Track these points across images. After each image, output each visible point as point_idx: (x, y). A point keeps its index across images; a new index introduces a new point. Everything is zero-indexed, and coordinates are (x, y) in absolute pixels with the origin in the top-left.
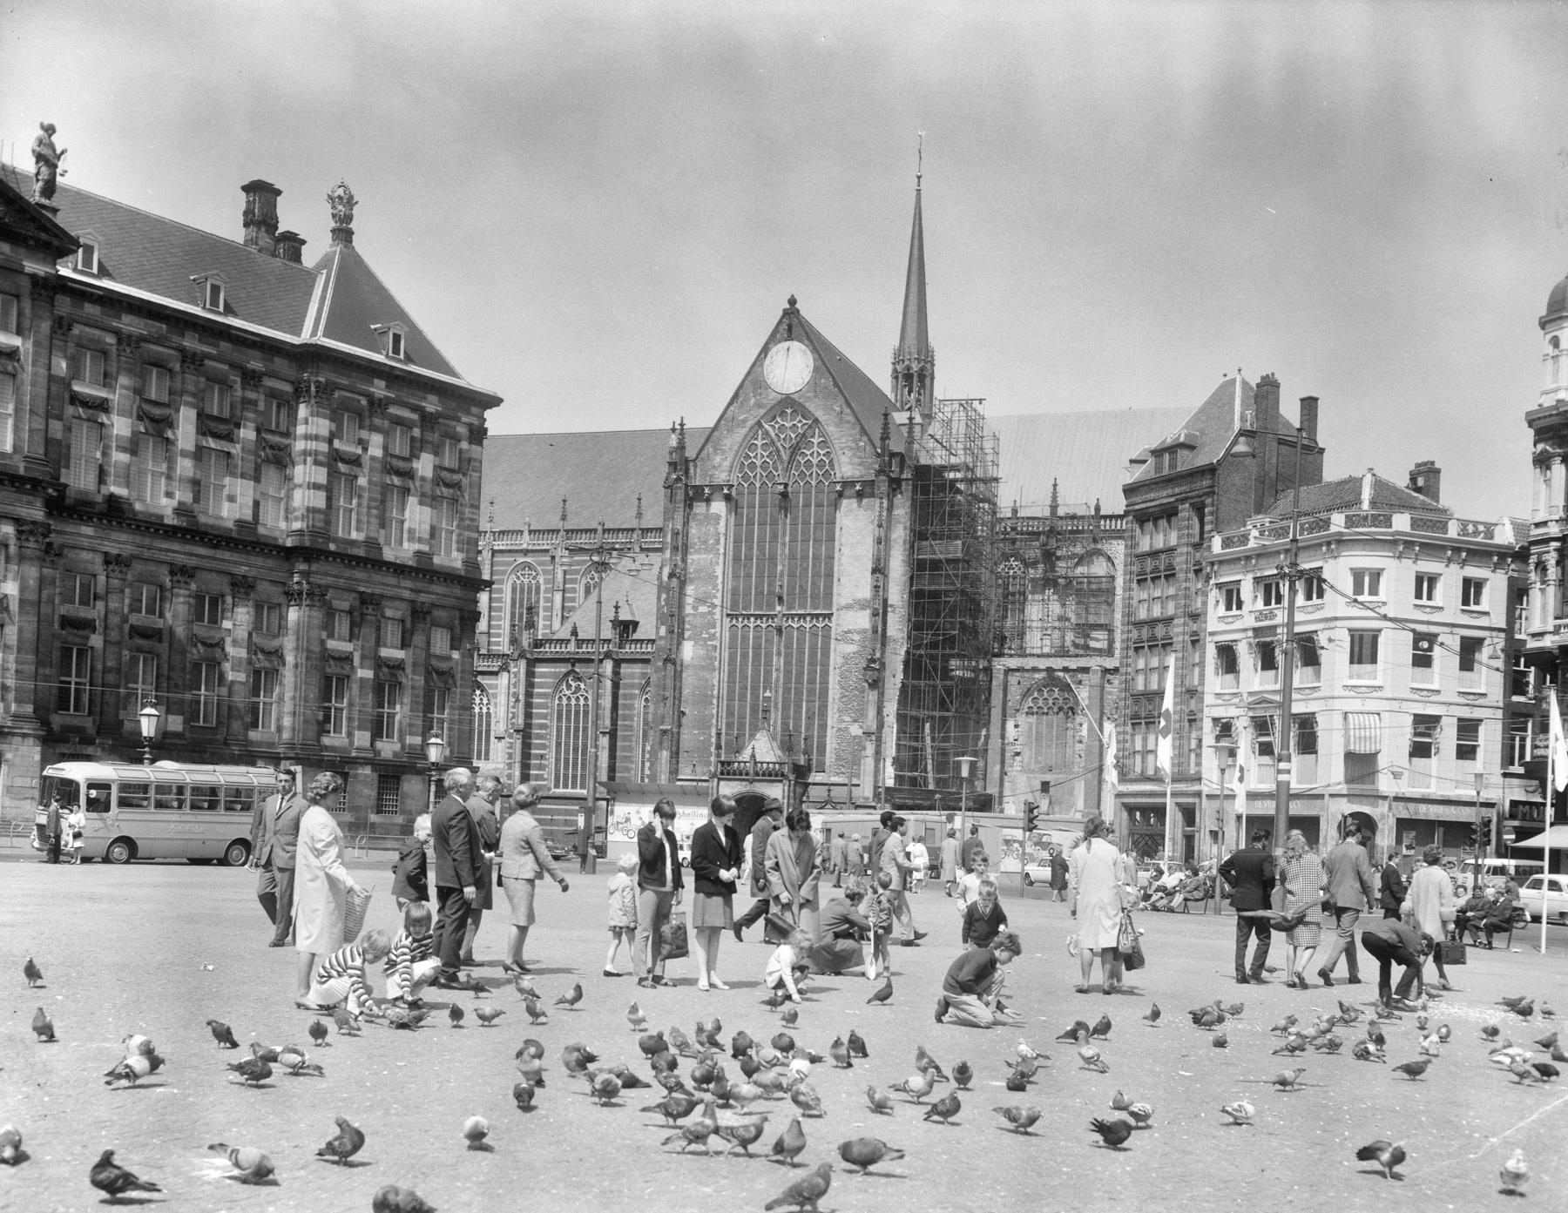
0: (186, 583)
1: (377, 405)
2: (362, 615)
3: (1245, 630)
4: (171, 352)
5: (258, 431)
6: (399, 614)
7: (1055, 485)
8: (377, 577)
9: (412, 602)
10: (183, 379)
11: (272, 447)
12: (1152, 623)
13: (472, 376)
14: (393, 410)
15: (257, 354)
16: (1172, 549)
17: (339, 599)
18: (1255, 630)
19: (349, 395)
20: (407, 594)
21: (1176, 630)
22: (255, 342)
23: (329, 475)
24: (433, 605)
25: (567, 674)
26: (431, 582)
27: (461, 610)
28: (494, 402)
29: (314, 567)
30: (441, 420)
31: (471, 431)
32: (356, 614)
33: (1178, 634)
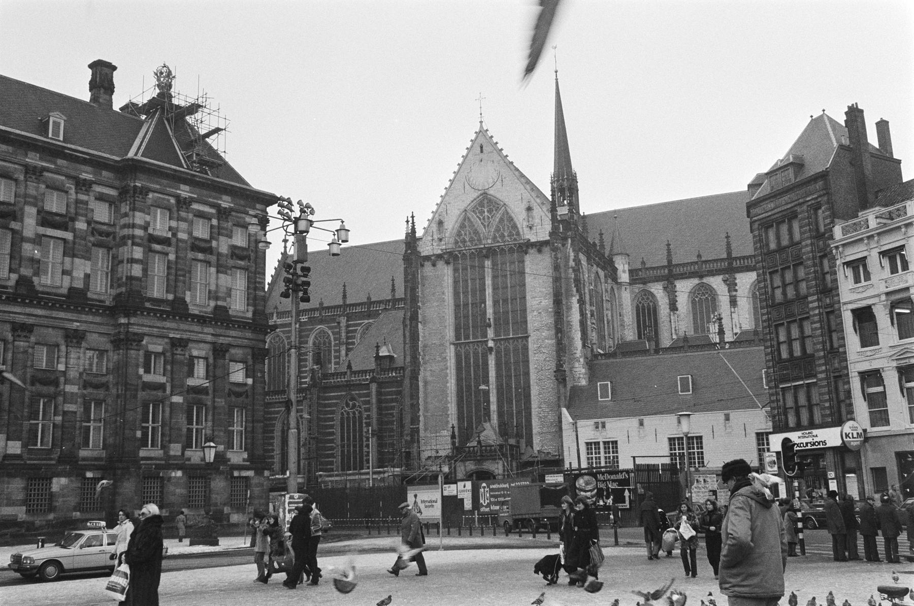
0: (25, 337)
1: (183, 203)
2: (173, 354)
3: (878, 296)
4: (16, 166)
5: (89, 223)
6: (203, 353)
7: (668, 245)
8: (183, 326)
9: (213, 343)
10: (26, 186)
11: (101, 234)
12: (787, 303)
13: (258, 182)
14: (195, 206)
15: (89, 169)
16: (799, 243)
17: (155, 344)
18: (887, 294)
19: (160, 195)
20: (209, 338)
21: (811, 305)
22: (85, 159)
23: (144, 253)
24: (230, 345)
26: (228, 328)
27: (253, 348)
29: (133, 320)
30: (233, 213)
32: (168, 354)
33: (814, 309)
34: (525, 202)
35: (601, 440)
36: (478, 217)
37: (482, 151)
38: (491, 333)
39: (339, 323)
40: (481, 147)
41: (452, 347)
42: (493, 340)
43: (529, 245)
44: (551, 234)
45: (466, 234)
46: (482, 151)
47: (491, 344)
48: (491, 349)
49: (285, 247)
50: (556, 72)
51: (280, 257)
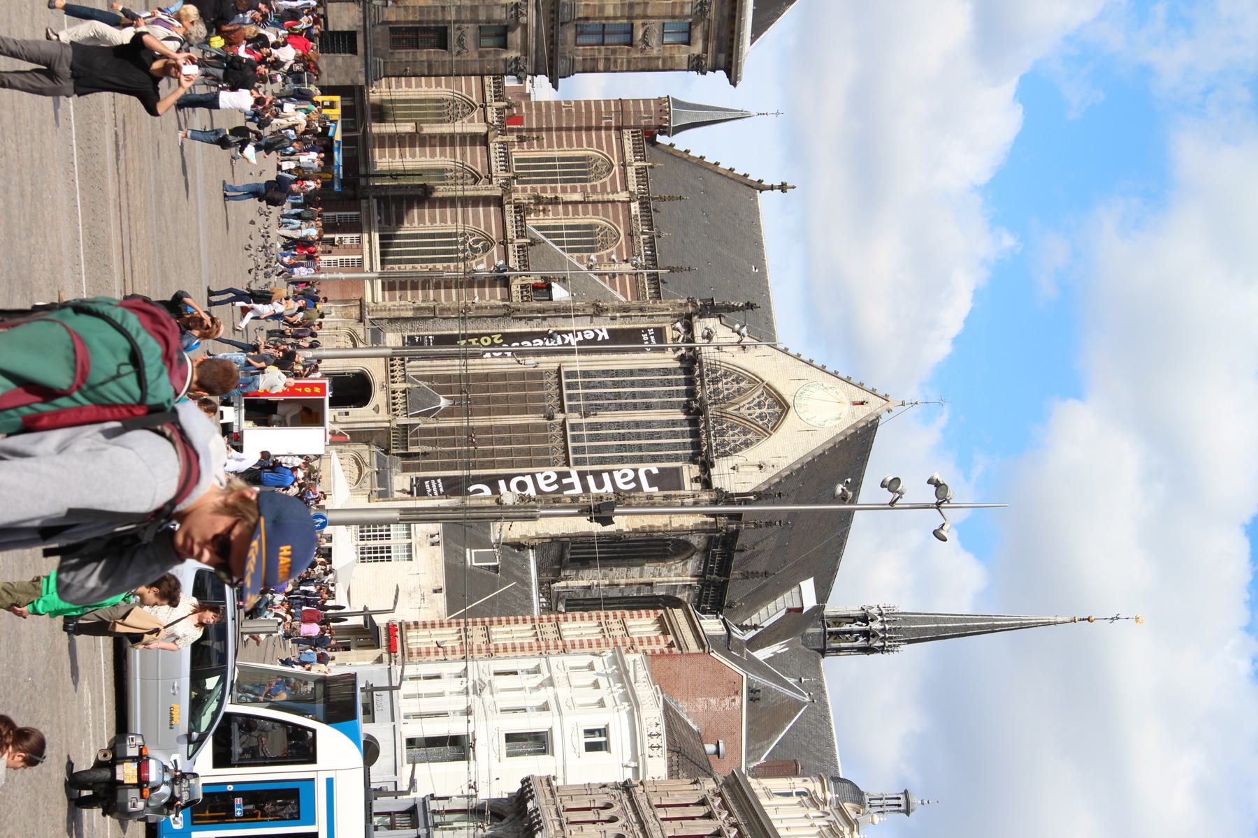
25: (488, 239)
28: (733, 80)
31: (698, 58)
34: (774, 461)
35: (413, 540)
36: (754, 399)
37: (855, 404)
38: (574, 418)
39: (627, 261)
40: (862, 403)
41: (557, 365)
42: (565, 420)
43: (706, 466)
44: (719, 491)
45: (726, 383)
46: (855, 404)
47: (559, 417)
48: (550, 418)
49: (772, 188)
50: (1088, 619)
51: (754, 177)
